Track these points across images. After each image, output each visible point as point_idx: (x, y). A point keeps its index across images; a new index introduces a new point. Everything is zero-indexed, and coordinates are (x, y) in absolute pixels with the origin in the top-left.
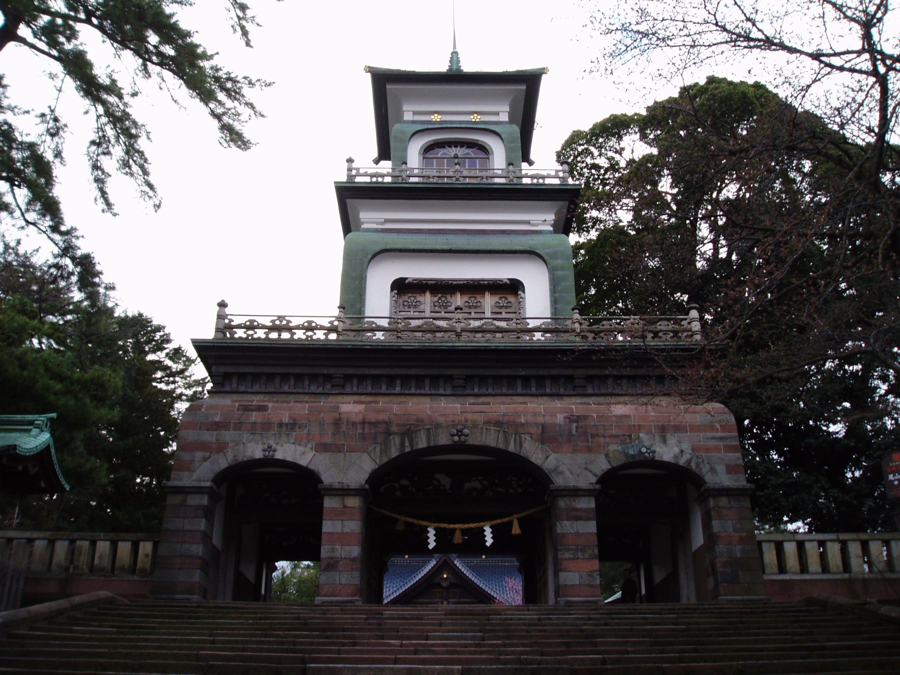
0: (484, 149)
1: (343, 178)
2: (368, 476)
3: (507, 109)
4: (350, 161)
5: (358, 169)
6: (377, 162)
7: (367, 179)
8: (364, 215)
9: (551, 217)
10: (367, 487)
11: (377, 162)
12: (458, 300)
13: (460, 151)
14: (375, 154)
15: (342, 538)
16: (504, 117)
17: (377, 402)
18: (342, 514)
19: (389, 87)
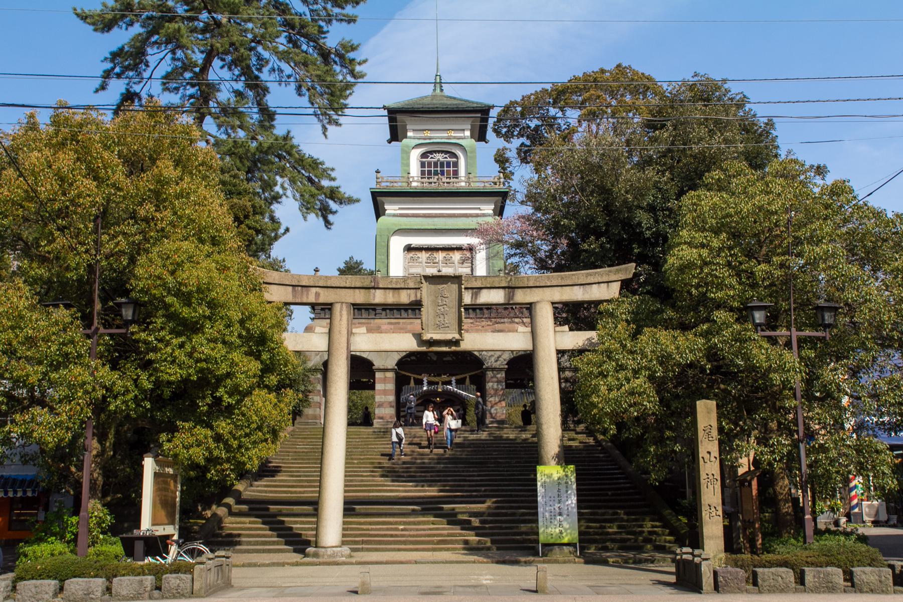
0: (454, 155)
1: (373, 185)
2: (396, 362)
3: (469, 127)
4: (378, 172)
5: (382, 178)
6: (390, 142)
7: (388, 184)
8: (386, 207)
9: (493, 207)
10: (396, 367)
11: (390, 142)
12: (440, 256)
13: (439, 157)
14: (389, 137)
15: (385, 392)
16: (468, 133)
17: (399, 323)
18: (385, 380)
19: (399, 117)
